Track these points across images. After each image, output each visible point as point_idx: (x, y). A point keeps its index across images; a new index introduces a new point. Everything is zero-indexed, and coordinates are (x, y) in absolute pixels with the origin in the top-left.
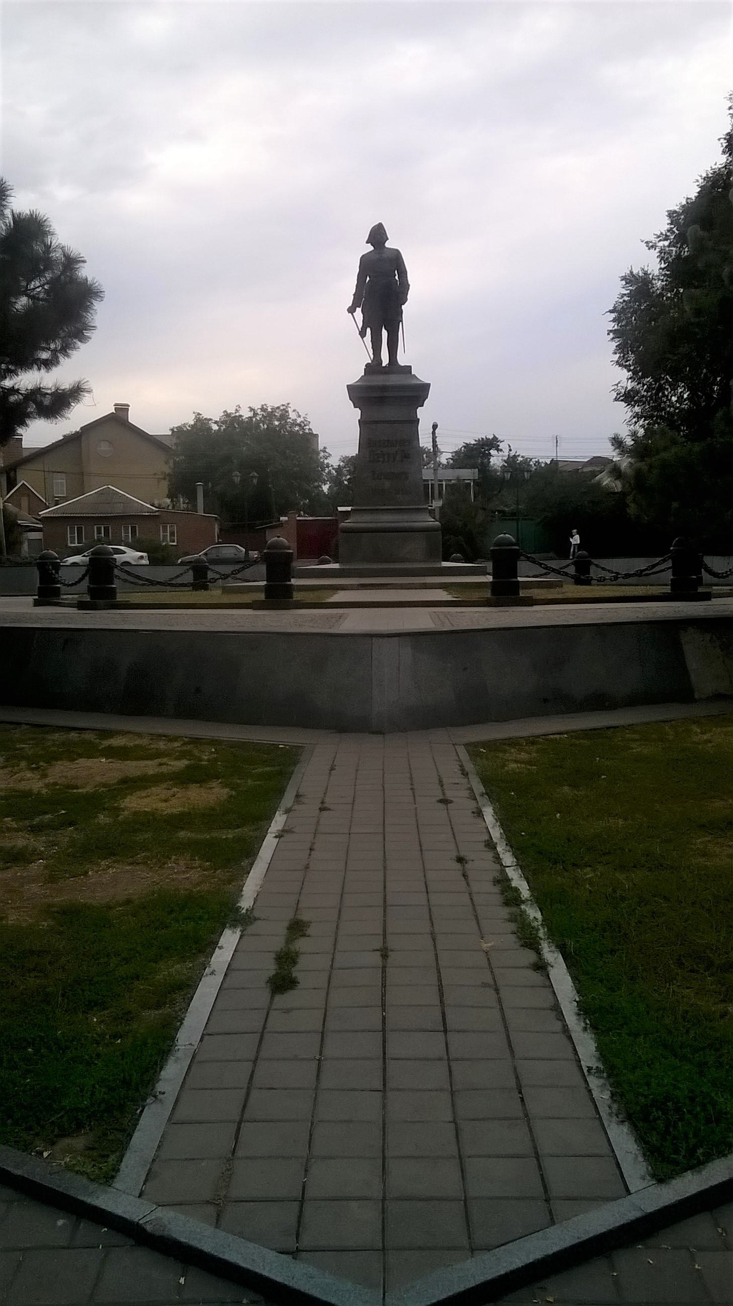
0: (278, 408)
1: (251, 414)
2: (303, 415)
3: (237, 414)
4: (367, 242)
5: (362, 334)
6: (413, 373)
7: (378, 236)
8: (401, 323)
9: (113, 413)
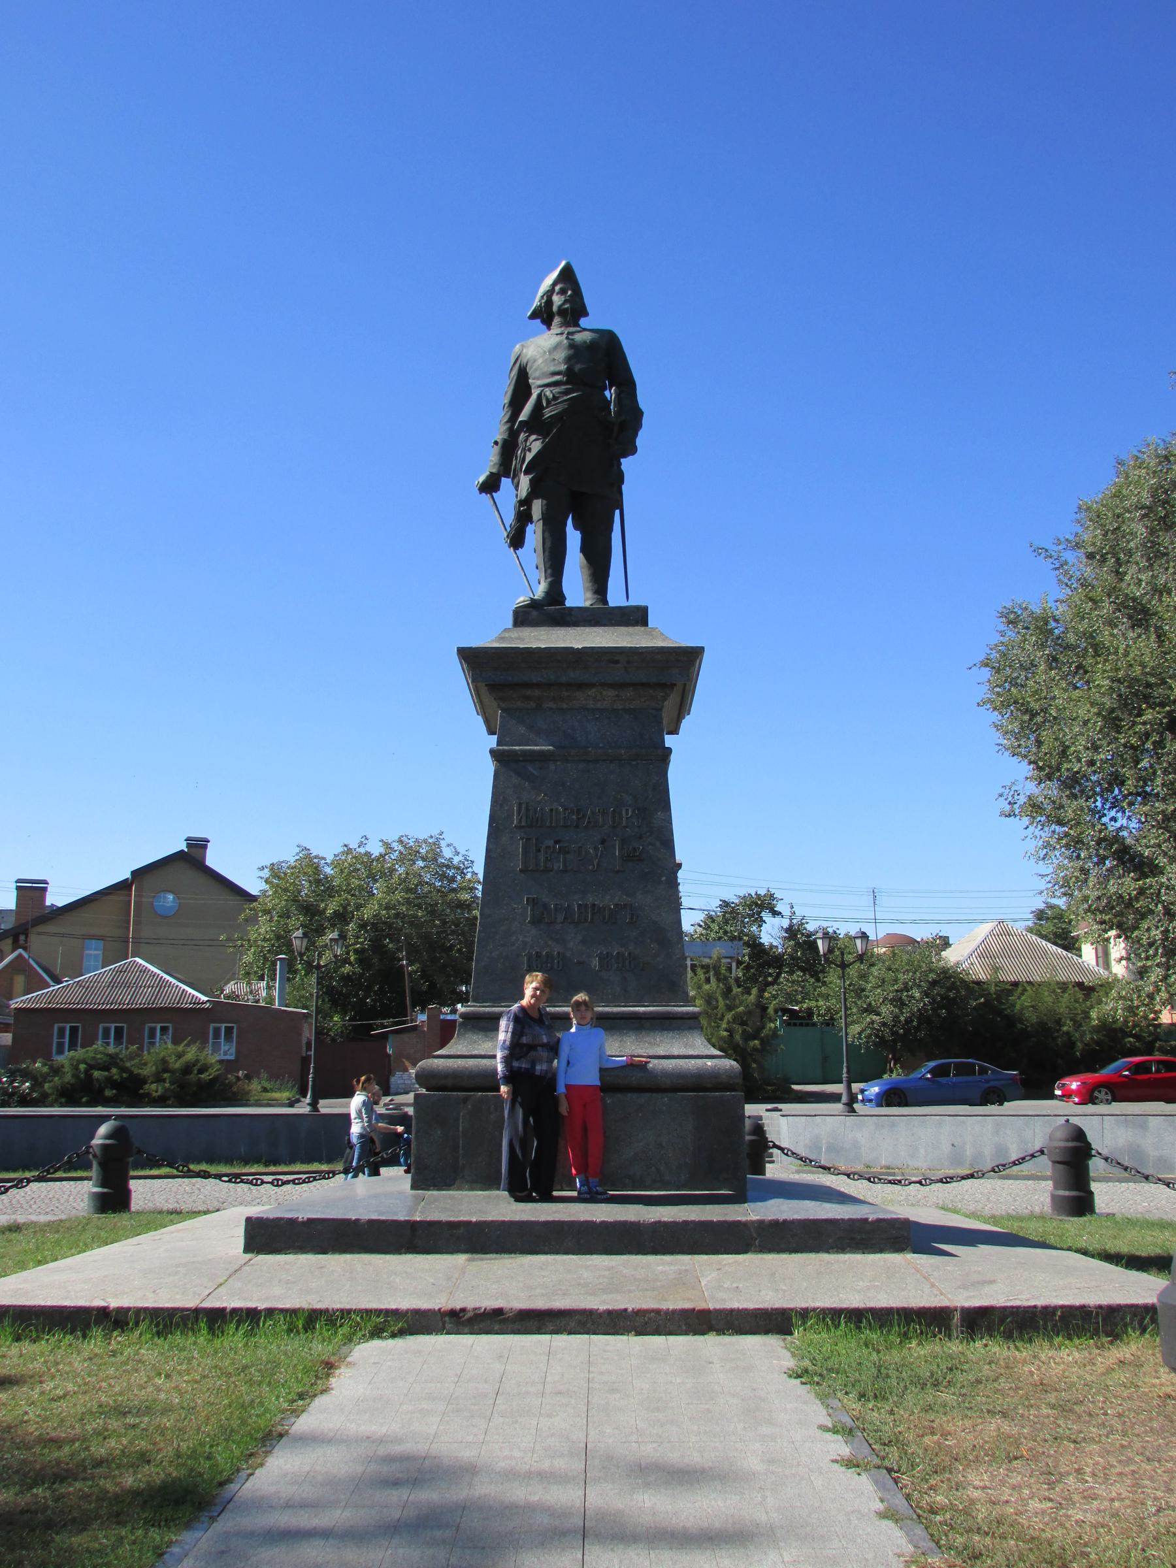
0: (425, 841)
1: (382, 850)
2: (463, 852)
3: (362, 850)
8: (617, 512)
9: (182, 851)
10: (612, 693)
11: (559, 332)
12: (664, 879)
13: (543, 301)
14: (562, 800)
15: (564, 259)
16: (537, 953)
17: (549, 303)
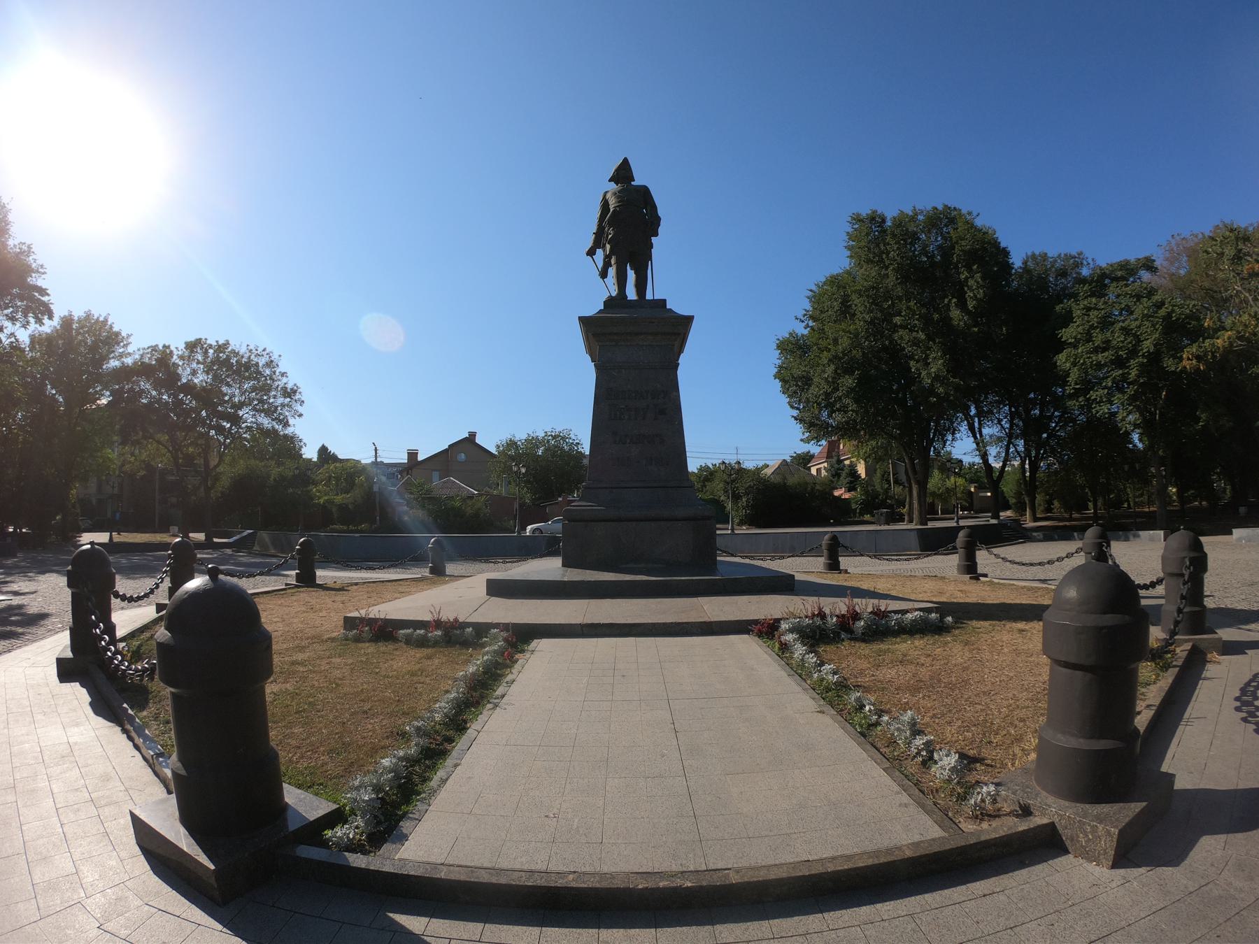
5: (604, 274)
6: (668, 307)
7: (623, 173)
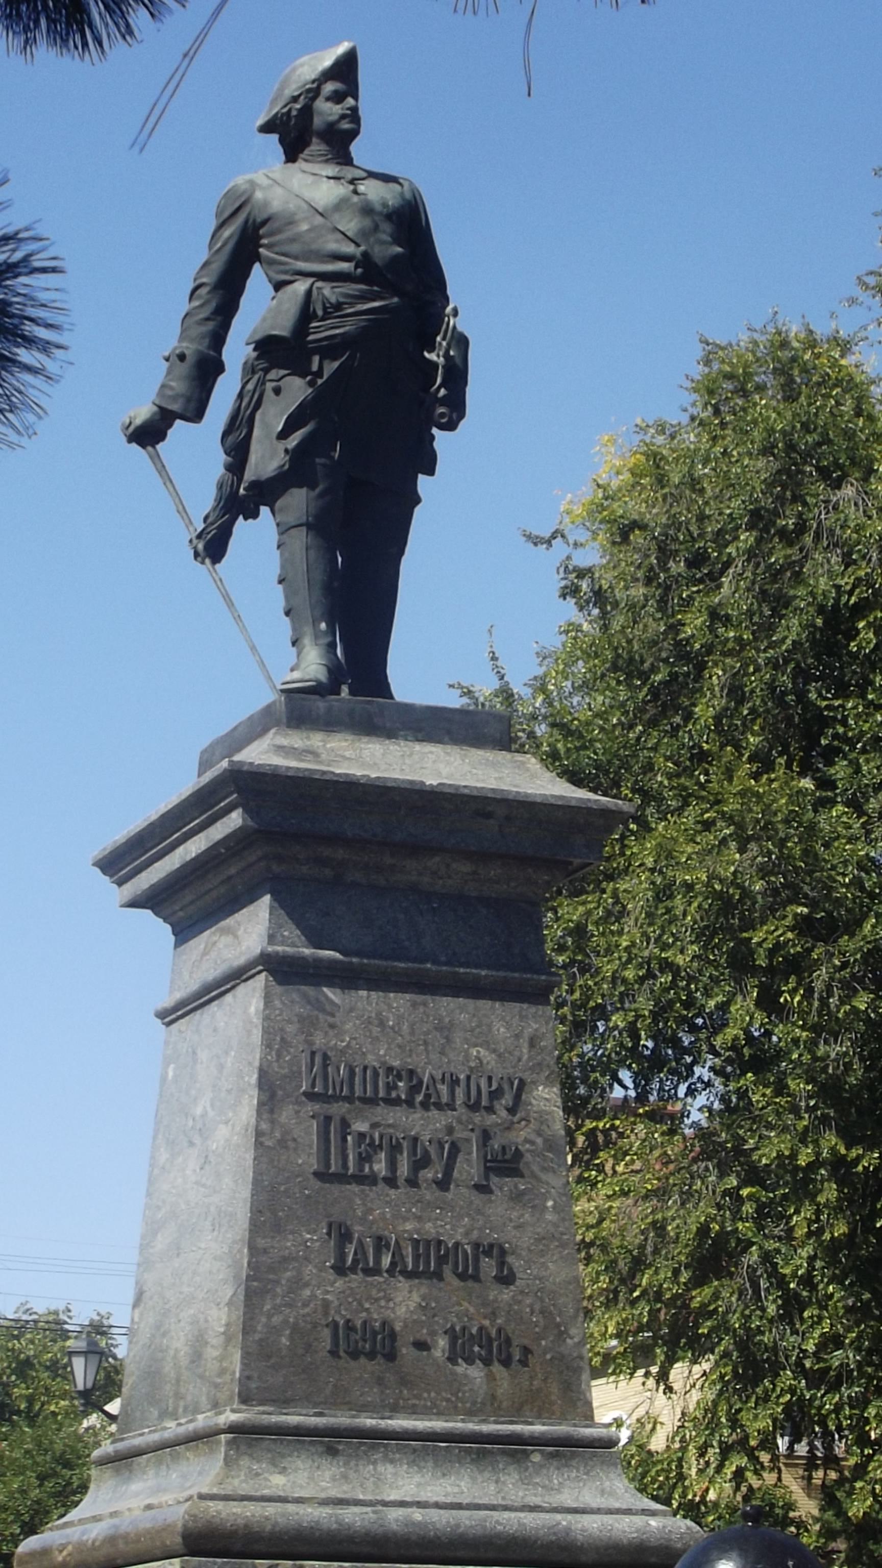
4: (267, 128)
10: (465, 867)
11: (330, 175)
12: (550, 1203)
13: (298, 106)
14: (382, 1052)
15: (349, 40)
16: (348, 1321)
17: (307, 112)
